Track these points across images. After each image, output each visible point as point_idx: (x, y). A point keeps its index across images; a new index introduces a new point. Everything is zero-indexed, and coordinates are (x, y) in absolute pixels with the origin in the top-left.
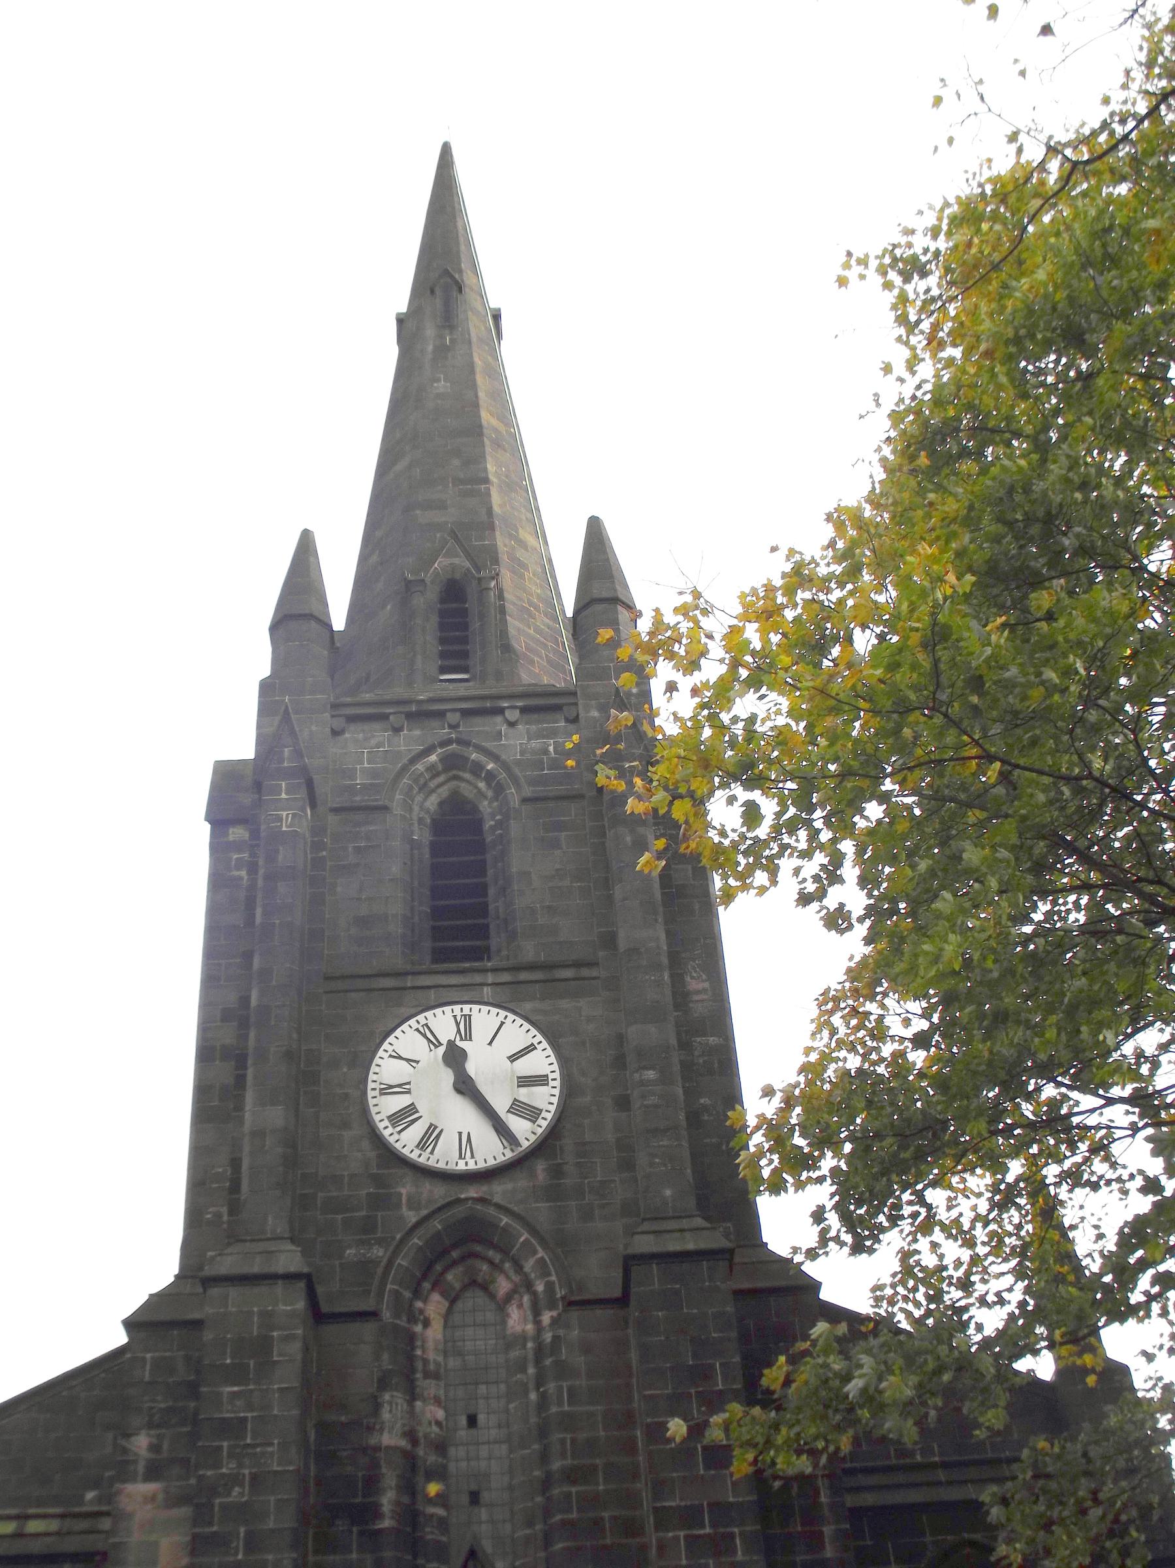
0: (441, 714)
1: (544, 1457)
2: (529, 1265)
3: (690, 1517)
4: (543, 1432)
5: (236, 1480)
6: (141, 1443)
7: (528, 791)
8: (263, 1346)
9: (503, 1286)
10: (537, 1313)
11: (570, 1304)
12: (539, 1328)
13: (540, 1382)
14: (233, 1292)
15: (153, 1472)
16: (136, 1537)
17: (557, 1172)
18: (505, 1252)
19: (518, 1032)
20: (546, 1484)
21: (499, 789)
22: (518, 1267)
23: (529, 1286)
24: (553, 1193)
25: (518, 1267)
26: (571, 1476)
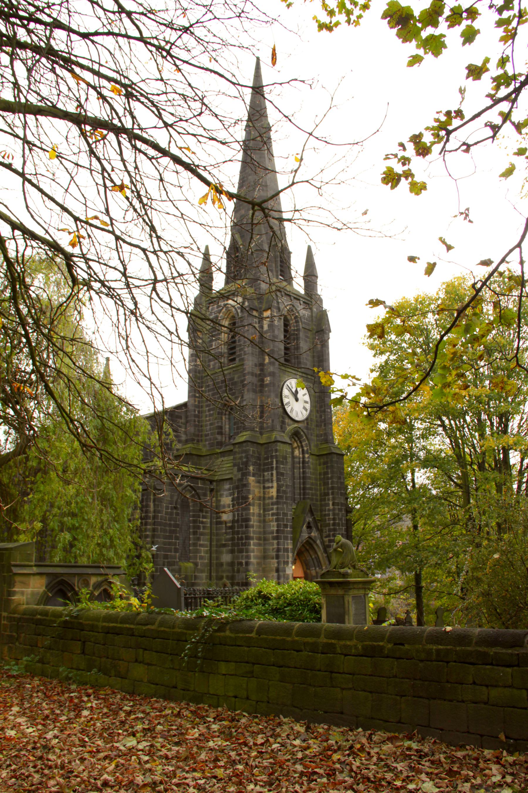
0: (290, 296)
1: (304, 483)
2: (303, 443)
3: (338, 504)
4: (304, 478)
5: (283, 485)
6: (251, 468)
7: (304, 326)
8: (285, 458)
9: (295, 445)
10: (303, 452)
11: (311, 454)
12: (304, 457)
13: (303, 468)
14: (282, 445)
15: (253, 476)
16: (252, 489)
17: (308, 424)
18: (299, 439)
19: (305, 391)
20: (304, 489)
21: (297, 322)
22: (301, 442)
23: (302, 447)
24: (307, 428)
25: (301, 442)
26: (311, 489)
